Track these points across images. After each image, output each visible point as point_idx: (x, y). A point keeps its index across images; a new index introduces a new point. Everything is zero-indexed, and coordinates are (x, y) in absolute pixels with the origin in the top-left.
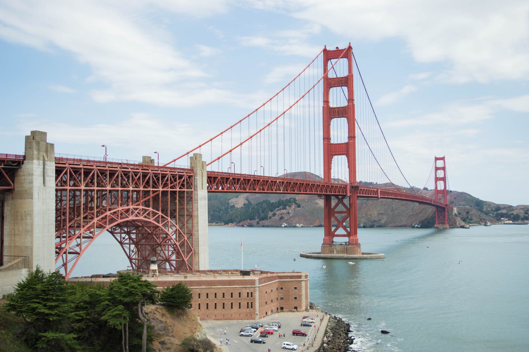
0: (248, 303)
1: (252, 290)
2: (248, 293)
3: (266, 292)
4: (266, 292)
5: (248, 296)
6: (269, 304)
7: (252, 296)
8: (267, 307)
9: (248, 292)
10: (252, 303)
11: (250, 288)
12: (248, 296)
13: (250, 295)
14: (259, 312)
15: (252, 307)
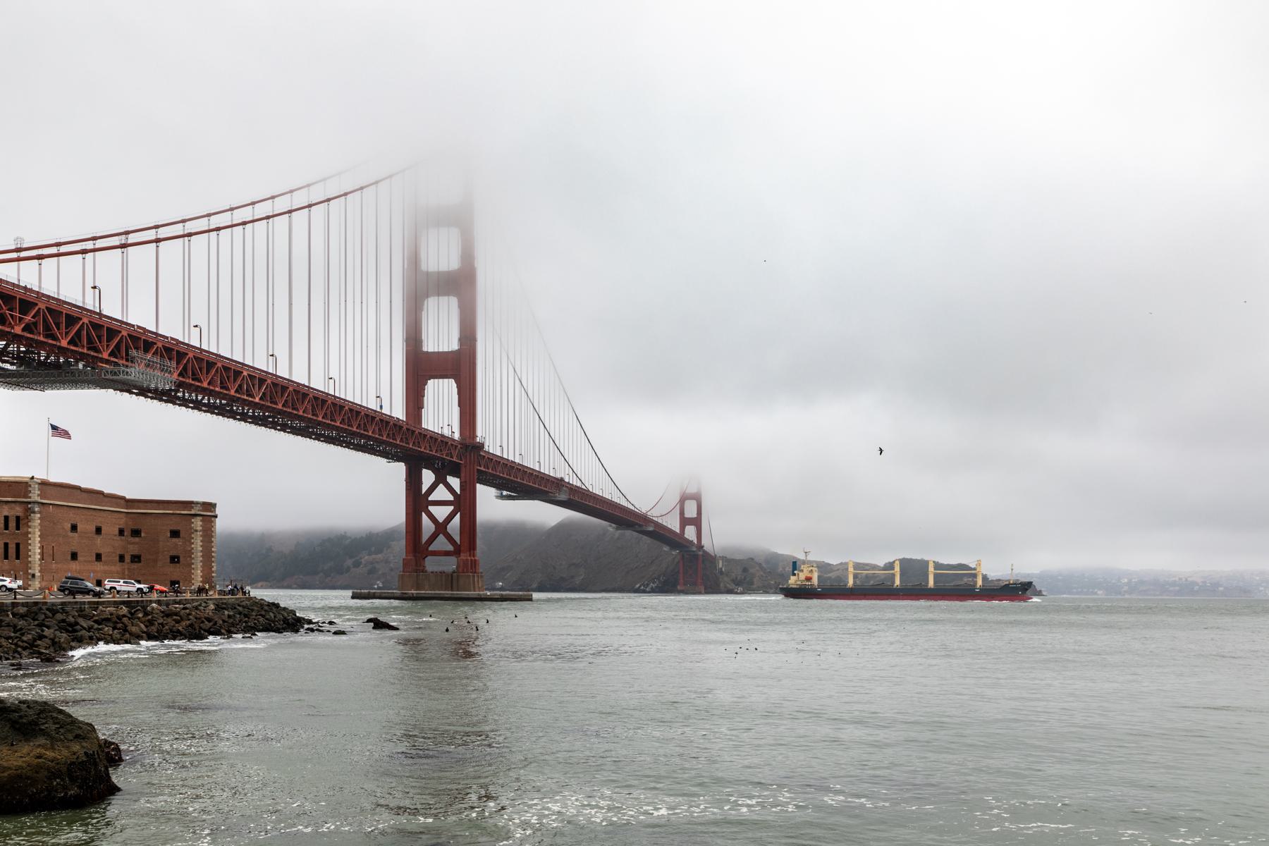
0: (6, 545)
1: (18, 511)
2: (6, 518)
3: (74, 528)
4: (74, 528)
5: (6, 527)
6: (85, 561)
7: (18, 528)
8: (74, 566)
9: (6, 513)
10: (18, 545)
11: (13, 505)
12: (6, 527)
13: (12, 524)
14: (40, 571)
15: (18, 558)
